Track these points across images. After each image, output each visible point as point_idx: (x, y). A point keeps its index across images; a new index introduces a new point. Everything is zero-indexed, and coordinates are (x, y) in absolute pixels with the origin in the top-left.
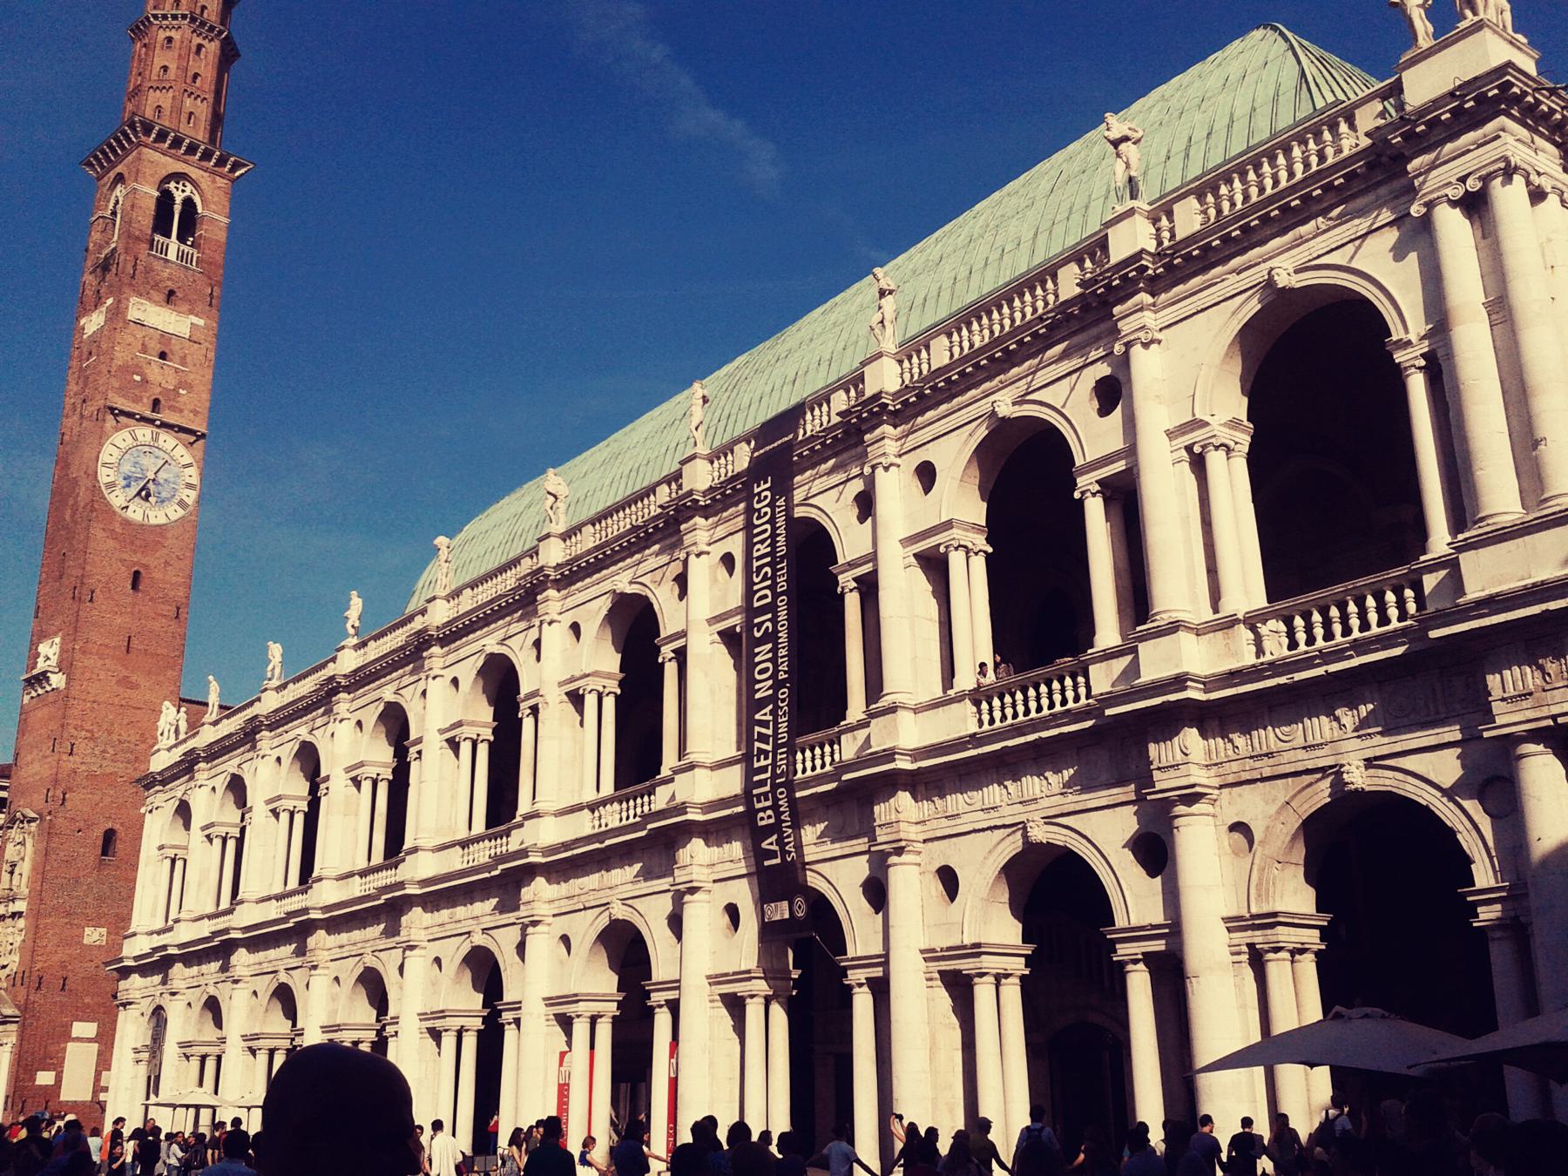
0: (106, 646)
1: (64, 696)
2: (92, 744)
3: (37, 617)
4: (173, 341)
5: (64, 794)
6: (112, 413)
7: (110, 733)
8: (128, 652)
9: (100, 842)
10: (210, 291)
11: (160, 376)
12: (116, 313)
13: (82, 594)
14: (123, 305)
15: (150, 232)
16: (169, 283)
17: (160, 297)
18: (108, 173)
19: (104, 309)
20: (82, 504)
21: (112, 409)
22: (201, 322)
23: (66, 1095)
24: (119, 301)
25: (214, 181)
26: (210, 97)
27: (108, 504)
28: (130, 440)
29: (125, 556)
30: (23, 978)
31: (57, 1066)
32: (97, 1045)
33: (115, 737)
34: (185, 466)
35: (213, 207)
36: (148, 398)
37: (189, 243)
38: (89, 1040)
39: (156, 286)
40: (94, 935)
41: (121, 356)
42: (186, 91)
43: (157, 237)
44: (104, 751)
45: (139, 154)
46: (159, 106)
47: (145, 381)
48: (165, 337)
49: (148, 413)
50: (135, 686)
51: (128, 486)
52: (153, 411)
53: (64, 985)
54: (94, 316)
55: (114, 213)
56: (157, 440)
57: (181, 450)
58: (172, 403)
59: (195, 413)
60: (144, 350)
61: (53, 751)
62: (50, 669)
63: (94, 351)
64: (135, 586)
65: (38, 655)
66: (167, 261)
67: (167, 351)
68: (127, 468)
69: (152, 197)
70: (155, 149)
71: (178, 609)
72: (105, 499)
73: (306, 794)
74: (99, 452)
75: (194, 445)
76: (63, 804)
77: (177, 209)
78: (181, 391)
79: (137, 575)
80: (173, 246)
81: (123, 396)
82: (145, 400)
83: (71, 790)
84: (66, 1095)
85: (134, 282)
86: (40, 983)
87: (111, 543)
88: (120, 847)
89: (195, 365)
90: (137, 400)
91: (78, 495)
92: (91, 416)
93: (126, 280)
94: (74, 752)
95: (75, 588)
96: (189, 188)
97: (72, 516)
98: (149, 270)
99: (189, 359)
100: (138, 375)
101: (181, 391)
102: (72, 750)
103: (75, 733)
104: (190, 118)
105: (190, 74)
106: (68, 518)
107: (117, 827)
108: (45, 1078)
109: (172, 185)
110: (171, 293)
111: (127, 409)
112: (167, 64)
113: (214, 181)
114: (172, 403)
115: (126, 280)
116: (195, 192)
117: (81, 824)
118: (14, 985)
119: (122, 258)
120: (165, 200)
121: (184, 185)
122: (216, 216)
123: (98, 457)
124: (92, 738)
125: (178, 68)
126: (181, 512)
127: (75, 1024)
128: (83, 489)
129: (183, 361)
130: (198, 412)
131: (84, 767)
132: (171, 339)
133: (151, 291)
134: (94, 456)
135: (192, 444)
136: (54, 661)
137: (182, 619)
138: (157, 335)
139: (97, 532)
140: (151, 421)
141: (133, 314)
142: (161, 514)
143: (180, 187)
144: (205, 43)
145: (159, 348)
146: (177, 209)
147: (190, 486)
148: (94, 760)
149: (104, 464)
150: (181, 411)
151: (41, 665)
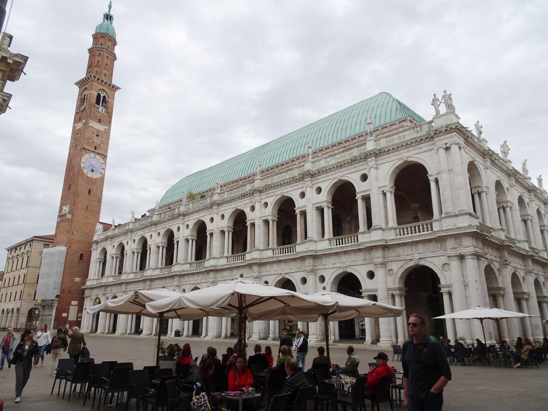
1: (71, 220)
2: (78, 232)
6: (85, 150)
7: (82, 230)
8: (87, 210)
9: (79, 257)
11: (97, 141)
12: (86, 124)
13: (76, 195)
14: (88, 122)
16: (99, 117)
17: (97, 121)
18: (82, 87)
20: (76, 172)
21: (85, 148)
23: (69, 319)
24: (87, 121)
27: (83, 173)
29: (87, 186)
31: (68, 312)
32: (77, 307)
33: (83, 231)
35: (110, 99)
38: (76, 305)
39: (96, 118)
40: (77, 280)
41: (87, 135)
43: (96, 105)
45: (92, 83)
47: (93, 142)
48: (98, 131)
49: (93, 150)
54: (79, 124)
55: (84, 98)
57: (101, 160)
60: (93, 134)
64: (89, 193)
65: (62, 209)
66: (99, 112)
68: (88, 163)
70: (96, 82)
73: (141, 248)
77: (102, 98)
79: (90, 190)
80: (101, 108)
83: (72, 244)
84: (69, 319)
87: (84, 182)
90: (91, 146)
96: (104, 93)
98: (94, 114)
99: (104, 136)
107: (83, 253)
108: (64, 315)
110: (100, 120)
117: (74, 252)
119: (88, 110)
120: (99, 95)
122: (111, 101)
124: (78, 231)
126: (101, 175)
127: (72, 301)
134: (80, 160)
136: (67, 211)
138: (96, 130)
139: (80, 179)
141: (90, 125)
142: (96, 176)
143: (102, 93)
144: (109, 55)
146: (102, 98)
148: (78, 236)
150: (101, 150)
151: (63, 212)
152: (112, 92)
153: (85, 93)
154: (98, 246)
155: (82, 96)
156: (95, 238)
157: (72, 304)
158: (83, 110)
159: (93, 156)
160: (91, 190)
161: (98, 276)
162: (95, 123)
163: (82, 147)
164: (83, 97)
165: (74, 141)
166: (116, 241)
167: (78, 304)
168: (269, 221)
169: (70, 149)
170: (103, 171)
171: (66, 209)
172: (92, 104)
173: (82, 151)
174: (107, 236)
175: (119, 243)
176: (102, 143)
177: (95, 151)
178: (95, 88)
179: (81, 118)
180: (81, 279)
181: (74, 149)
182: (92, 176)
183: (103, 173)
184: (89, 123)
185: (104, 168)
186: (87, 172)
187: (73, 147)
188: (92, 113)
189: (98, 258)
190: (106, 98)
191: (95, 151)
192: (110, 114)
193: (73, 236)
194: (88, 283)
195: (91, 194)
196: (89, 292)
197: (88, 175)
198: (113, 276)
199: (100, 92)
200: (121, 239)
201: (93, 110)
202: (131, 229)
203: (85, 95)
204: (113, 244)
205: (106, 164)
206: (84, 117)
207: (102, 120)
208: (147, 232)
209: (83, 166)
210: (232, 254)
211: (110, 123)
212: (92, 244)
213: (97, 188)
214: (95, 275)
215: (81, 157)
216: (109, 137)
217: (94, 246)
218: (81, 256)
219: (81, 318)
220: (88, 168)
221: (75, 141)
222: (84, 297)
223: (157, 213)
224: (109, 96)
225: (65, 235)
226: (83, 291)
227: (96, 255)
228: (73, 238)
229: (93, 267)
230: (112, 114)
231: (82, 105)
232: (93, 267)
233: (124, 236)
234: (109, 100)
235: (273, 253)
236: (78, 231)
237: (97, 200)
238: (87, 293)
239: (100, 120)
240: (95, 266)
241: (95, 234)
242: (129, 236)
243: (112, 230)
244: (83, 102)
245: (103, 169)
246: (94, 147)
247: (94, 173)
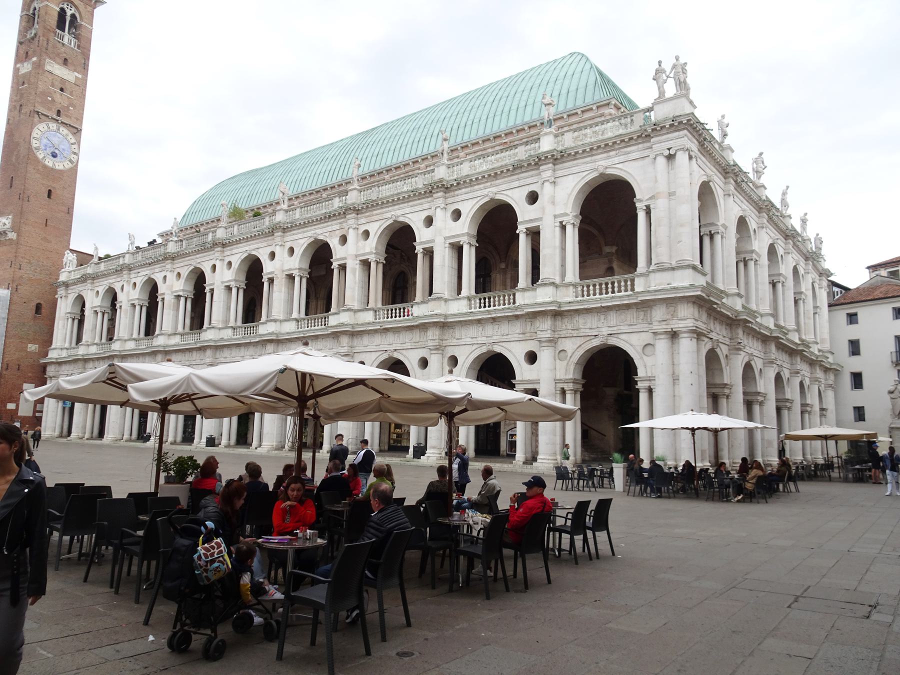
1: (17, 243)
2: (30, 266)
6: (38, 115)
7: (38, 261)
10: (83, 61)
11: (61, 100)
12: (39, 66)
16: (65, 55)
17: (61, 61)
20: (22, 155)
21: (38, 112)
22: (80, 76)
24: (40, 60)
25: (86, 8)
27: (36, 157)
28: (46, 128)
29: (44, 182)
31: (17, 401)
33: (41, 263)
34: (72, 144)
39: (58, 55)
40: (33, 347)
41: (41, 87)
43: (58, 31)
47: (53, 100)
48: (63, 81)
49: (55, 116)
50: (49, 242)
54: (25, 64)
55: (34, 14)
57: (71, 136)
58: (66, 113)
60: (53, 86)
64: (49, 196)
66: (63, 44)
68: (45, 141)
69: (56, 10)
74: (31, 132)
75: (77, 134)
76: (17, 290)
77: (68, 19)
79: (50, 191)
81: (43, 107)
83: (20, 284)
90: (50, 109)
92: (26, 113)
93: (44, 50)
94: (22, 268)
98: (54, 47)
99: (74, 93)
106: (14, 160)
108: (11, 406)
110: (66, 60)
111: (45, 113)
114: (66, 113)
117: (25, 300)
119: (41, 38)
122: (87, 25)
123: (31, 134)
124: (30, 263)
126: (70, 165)
127: (24, 384)
129: (71, 94)
131: (26, 275)
136: (8, 226)
138: (59, 79)
139: (30, 169)
141: (48, 67)
145: (60, 86)
146: (68, 19)
148: (31, 272)
150: (70, 118)
152: (89, 8)
153: (36, 5)
154: (69, 292)
155: (29, 10)
156: (63, 277)
158: (33, 39)
159: (55, 128)
160: (52, 190)
161: (71, 343)
162: (57, 66)
164: (31, 12)
165: (16, 96)
166: (101, 284)
168: (370, 263)
169: (10, 110)
170: (75, 156)
171: (7, 222)
172: (49, 27)
173: (34, 117)
174: (85, 275)
175: (108, 287)
177: (58, 118)
179: (29, 53)
180: (39, 347)
181: (17, 112)
183: (74, 160)
185: (76, 151)
186: (44, 157)
187: (15, 107)
188: (50, 45)
189: (69, 313)
190: (76, 18)
191: (58, 118)
192: (85, 51)
193: (20, 271)
194: (53, 355)
196: (55, 369)
197: (46, 163)
198: (97, 344)
199: (65, 6)
200: (111, 281)
201: (51, 39)
202: (129, 265)
203: (35, 9)
204: (96, 289)
205: (79, 145)
206: (34, 51)
207: (69, 61)
208: (157, 270)
209: (34, 145)
210: (306, 315)
211: (85, 68)
212: (57, 287)
214: (65, 341)
216: (85, 95)
217: (61, 291)
218: (38, 308)
219: (42, 412)
220: (46, 150)
221: (18, 97)
222: (46, 378)
223: (176, 239)
224: (83, 15)
225: (5, 269)
226: (44, 368)
227: (65, 307)
229: (60, 326)
230: (89, 51)
231: (30, 28)
232: (60, 326)
233: (115, 276)
234: (83, 23)
235: (376, 316)
236: (30, 263)
237: (65, 209)
238: (51, 371)
239: (66, 60)
240: (64, 326)
241: (63, 270)
242: (125, 276)
243: (93, 265)
244: (31, 23)
245: (75, 153)
246: (56, 112)
247: (58, 159)
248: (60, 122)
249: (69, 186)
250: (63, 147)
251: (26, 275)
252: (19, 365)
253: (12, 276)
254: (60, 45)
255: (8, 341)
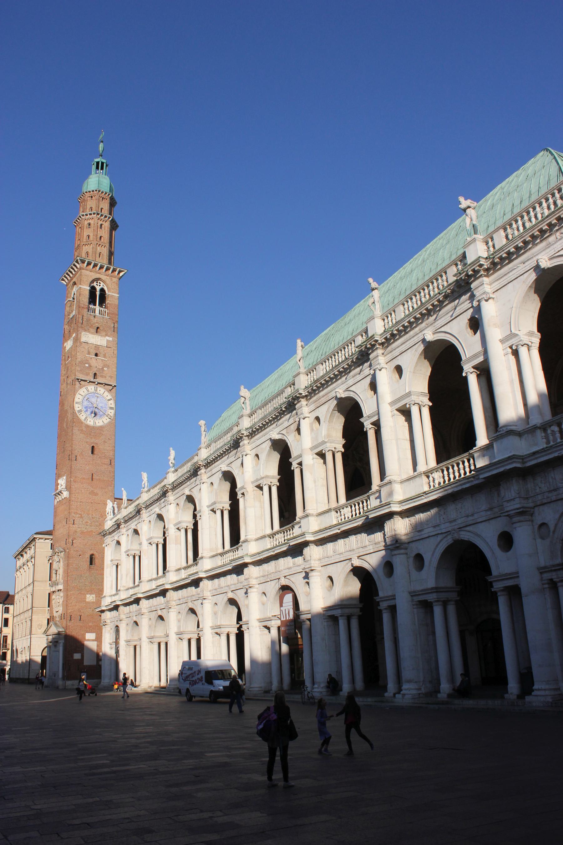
0: (84, 478)
2: (81, 520)
3: (57, 469)
4: (100, 348)
5: (73, 541)
9: (89, 560)
11: (96, 363)
12: (77, 340)
13: (73, 458)
14: (79, 336)
15: (87, 304)
16: (97, 324)
17: (95, 330)
19: (72, 338)
21: (78, 379)
22: (111, 339)
23: (86, 663)
25: (112, 280)
26: (108, 245)
27: (79, 419)
29: (88, 440)
30: (64, 616)
32: (96, 642)
34: (109, 400)
36: (92, 373)
37: (104, 307)
38: (93, 640)
39: (91, 326)
41: (80, 357)
42: (97, 244)
43: (92, 306)
44: (87, 522)
45: (81, 273)
46: (88, 252)
47: (90, 366)
48: (97, 347)
49: (92, 380)
51: (87, 411)
52: (94, 378)
53: (80, 618)
54: (69, 342)
55: (74, 299)
56: (96, 390)
57: (106, 393)
59: (111, 377)
60: (89, 353)
61: (67, 523)
62: (63, 490)
63: (70, 356)
64: (93, 452)
65: (58, 484)
67: (98, 352)
68: (86, 403)
69: (87, 289)
71: (111, 461)
72: (78, 417)
74: (74, 398)
77: (98, 293)
78: (105, 369)
79: (93, 447)
80: (97, 308)
82: (91, 374)
83: (75, 539)
84: (86, 663)
85: (83, 326)
86: (71, 618)
87: (82, 435)
88: (97, 561)
89: (109, 357)
90: (87, 374)
91: (68, 416)
93: (80, 325)
95: (69, 455)
96: (102, 284)
97: (67, 426)
98: (88, 320)
99: (107, 355)
100: (87, 364)
101: (105, 369)
102: (74, 522)
103: (75, 515)
104: (100, 255)
105: (99, 237)
107: (95, 553)
108: (77, 656)
109: (95, 284)
111: (83, 379)
112: (88, 234)
113: (112, 280)
115: (80, 325)
116: (104, 285)
117: (81, 553)
118: (61, 619)
120: (93, 290)
121: (100, 283)
123: (74, 400)
124: (81, 517)
125: (93, 235)
128: (70, 413)
129: (105, 356)
130: (112, 377)
131: (79, 529)
132: (99, 347)
133: (90, 329)
135: (110, 390)
136: (64, 486)
137: (112, 465)
139: (76, 430)
140: (94, 382)
141: (83, 339)
142: (101, 422)
143: (98, 284)
144: (104, 223)
145: (94, 352)
146: (98, 293)
147: (111, 408)
149: (77, 403)
157: (87, 638)
160: (96, 447)
162: (91, 336)
163: (73, 377)
167: (96, 638)
172: (82, 306)
176: (105, 366)
177: (95, 380)
178: (85, 280)
179: (71, 331)
180: (96, 596)
182: (95, 423)
184: (81, 337)
186: (86, 418)
195: (95, 453)
199: (95, 284)
201: (85, 315)
206: (74, 329)
207: (101, 328)
213: (105, 442)
215: (75, 395)
221: (66, 371)
223: (173, 469)
225: (64, 526)
228: (74, 529)
236: (81, 517)
246: (93, 376)
247: (98, 417)
248: (96, 383)
249: (109, 439)
250: (101, 405)
251: (79, 529)
252: (80, 616)
253: (68, 531)
254: (92, 318)
255: (69, 593)
